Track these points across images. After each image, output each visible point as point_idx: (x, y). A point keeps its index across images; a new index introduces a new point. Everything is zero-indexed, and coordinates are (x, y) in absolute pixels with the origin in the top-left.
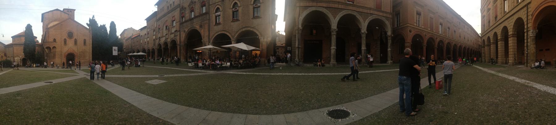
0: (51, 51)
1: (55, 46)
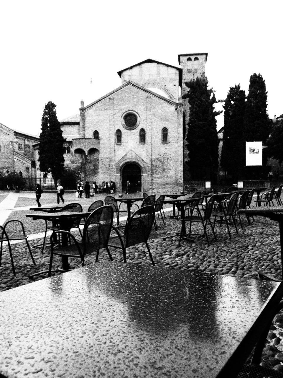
0: (88, 158)
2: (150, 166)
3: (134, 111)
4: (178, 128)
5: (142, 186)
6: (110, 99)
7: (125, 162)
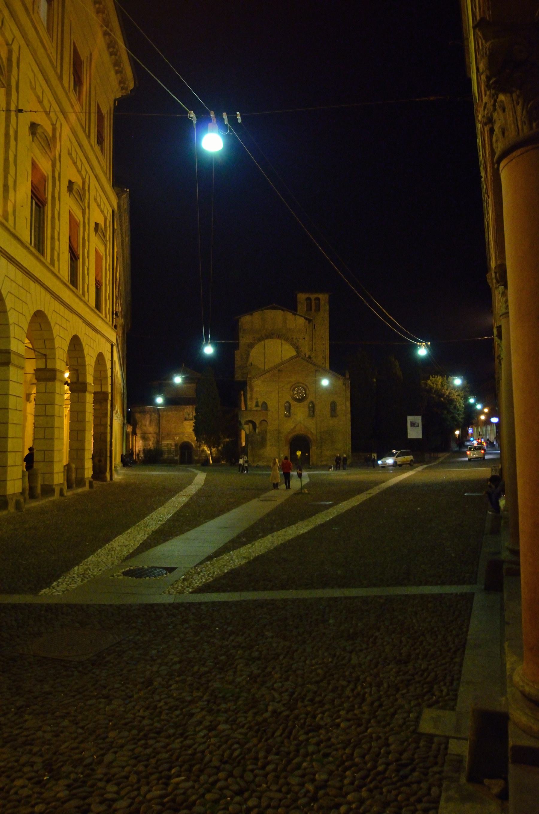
1: (265, 419)
2: (319, 438)
3: (303, 384)
4: (346, 402)
5: (311, 458)
6: (279, 370)
7: (294, 434)
